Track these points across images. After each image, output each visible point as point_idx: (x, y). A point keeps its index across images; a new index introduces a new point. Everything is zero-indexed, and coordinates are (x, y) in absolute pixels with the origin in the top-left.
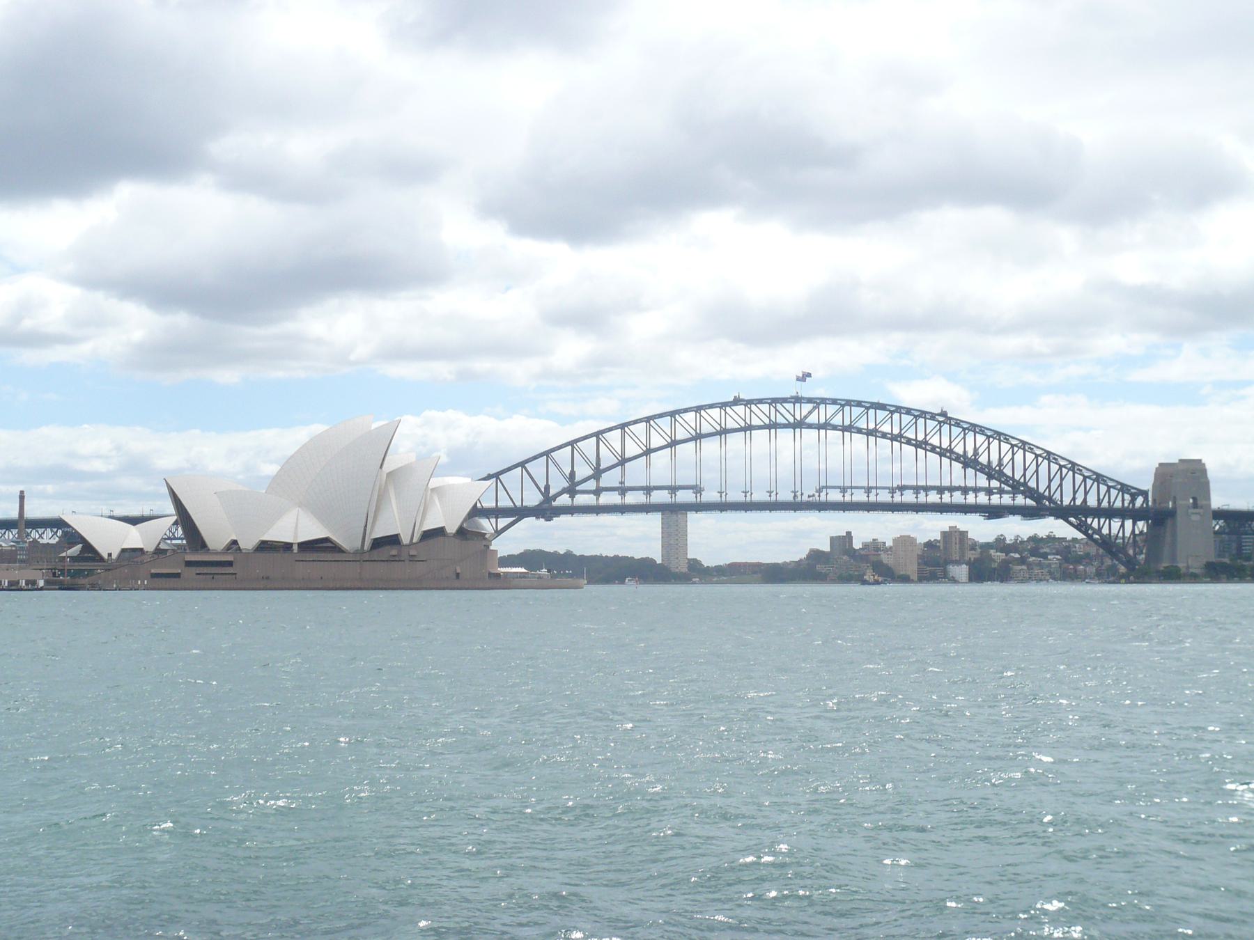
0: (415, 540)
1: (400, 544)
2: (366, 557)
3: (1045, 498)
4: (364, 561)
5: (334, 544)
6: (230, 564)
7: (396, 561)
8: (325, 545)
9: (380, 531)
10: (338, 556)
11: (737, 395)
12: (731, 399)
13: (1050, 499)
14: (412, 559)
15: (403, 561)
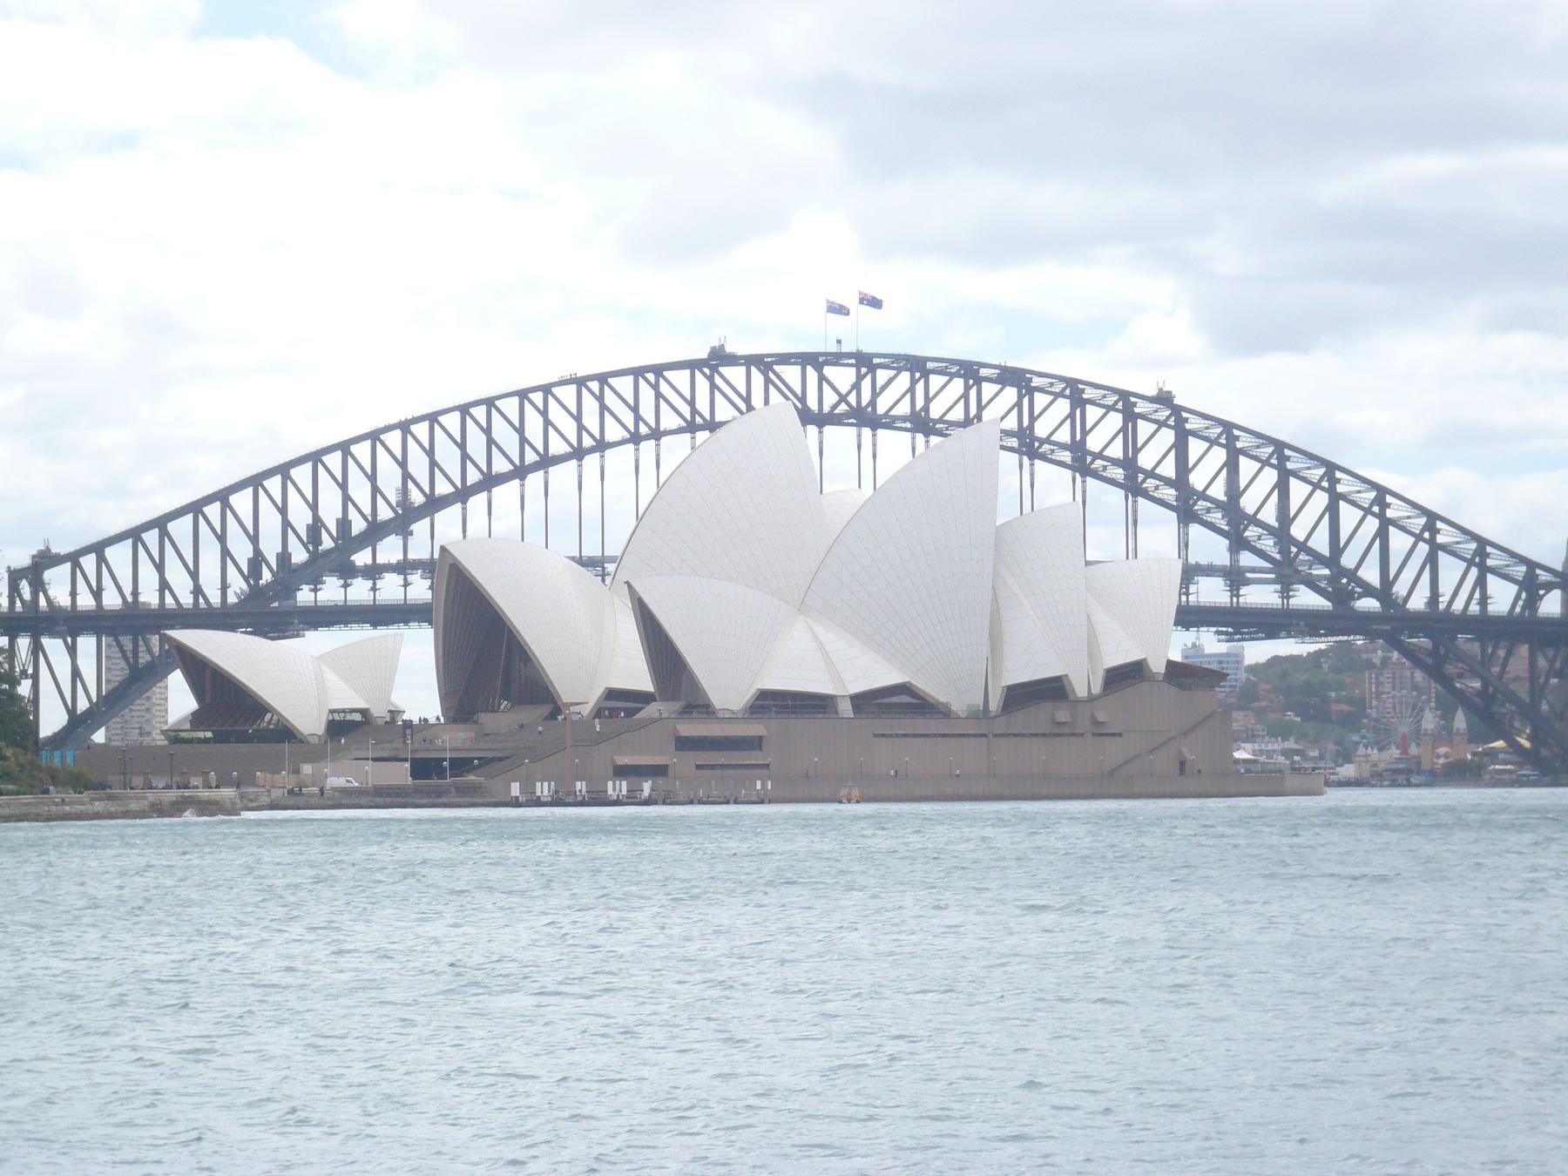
0: (1097, 689)
1: (1071, 697)
2: (1000, 726)
3: (1368, 591)
4: (996, 735)
5: (925, 700)
6: (755, 743)
7: (1063, 735)
8: (895, 699)
9: (1019, 671)
10: (933, 725)
11: (716, 344)
12: (704, 355)
13: (1384, 592)
14: (1100, 732)
15: (1082, 735)
